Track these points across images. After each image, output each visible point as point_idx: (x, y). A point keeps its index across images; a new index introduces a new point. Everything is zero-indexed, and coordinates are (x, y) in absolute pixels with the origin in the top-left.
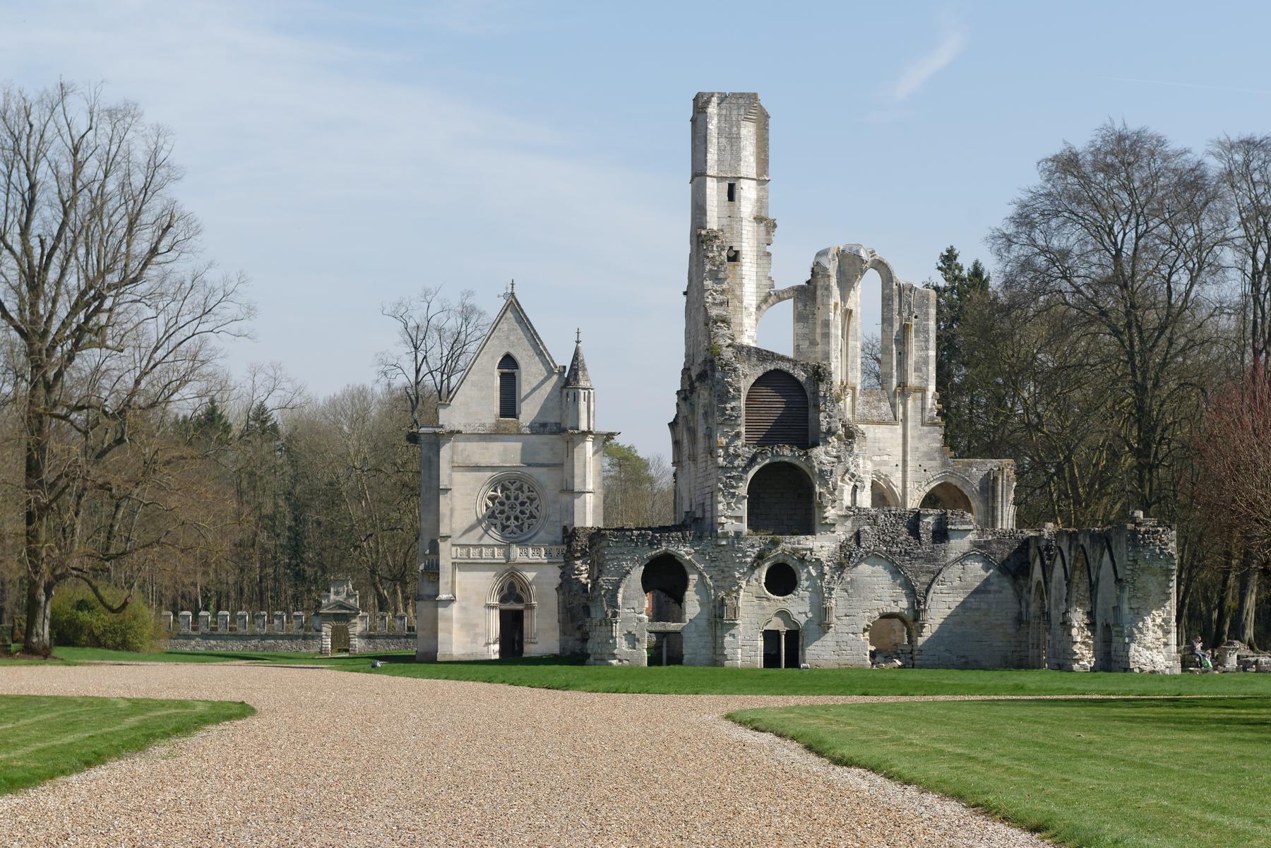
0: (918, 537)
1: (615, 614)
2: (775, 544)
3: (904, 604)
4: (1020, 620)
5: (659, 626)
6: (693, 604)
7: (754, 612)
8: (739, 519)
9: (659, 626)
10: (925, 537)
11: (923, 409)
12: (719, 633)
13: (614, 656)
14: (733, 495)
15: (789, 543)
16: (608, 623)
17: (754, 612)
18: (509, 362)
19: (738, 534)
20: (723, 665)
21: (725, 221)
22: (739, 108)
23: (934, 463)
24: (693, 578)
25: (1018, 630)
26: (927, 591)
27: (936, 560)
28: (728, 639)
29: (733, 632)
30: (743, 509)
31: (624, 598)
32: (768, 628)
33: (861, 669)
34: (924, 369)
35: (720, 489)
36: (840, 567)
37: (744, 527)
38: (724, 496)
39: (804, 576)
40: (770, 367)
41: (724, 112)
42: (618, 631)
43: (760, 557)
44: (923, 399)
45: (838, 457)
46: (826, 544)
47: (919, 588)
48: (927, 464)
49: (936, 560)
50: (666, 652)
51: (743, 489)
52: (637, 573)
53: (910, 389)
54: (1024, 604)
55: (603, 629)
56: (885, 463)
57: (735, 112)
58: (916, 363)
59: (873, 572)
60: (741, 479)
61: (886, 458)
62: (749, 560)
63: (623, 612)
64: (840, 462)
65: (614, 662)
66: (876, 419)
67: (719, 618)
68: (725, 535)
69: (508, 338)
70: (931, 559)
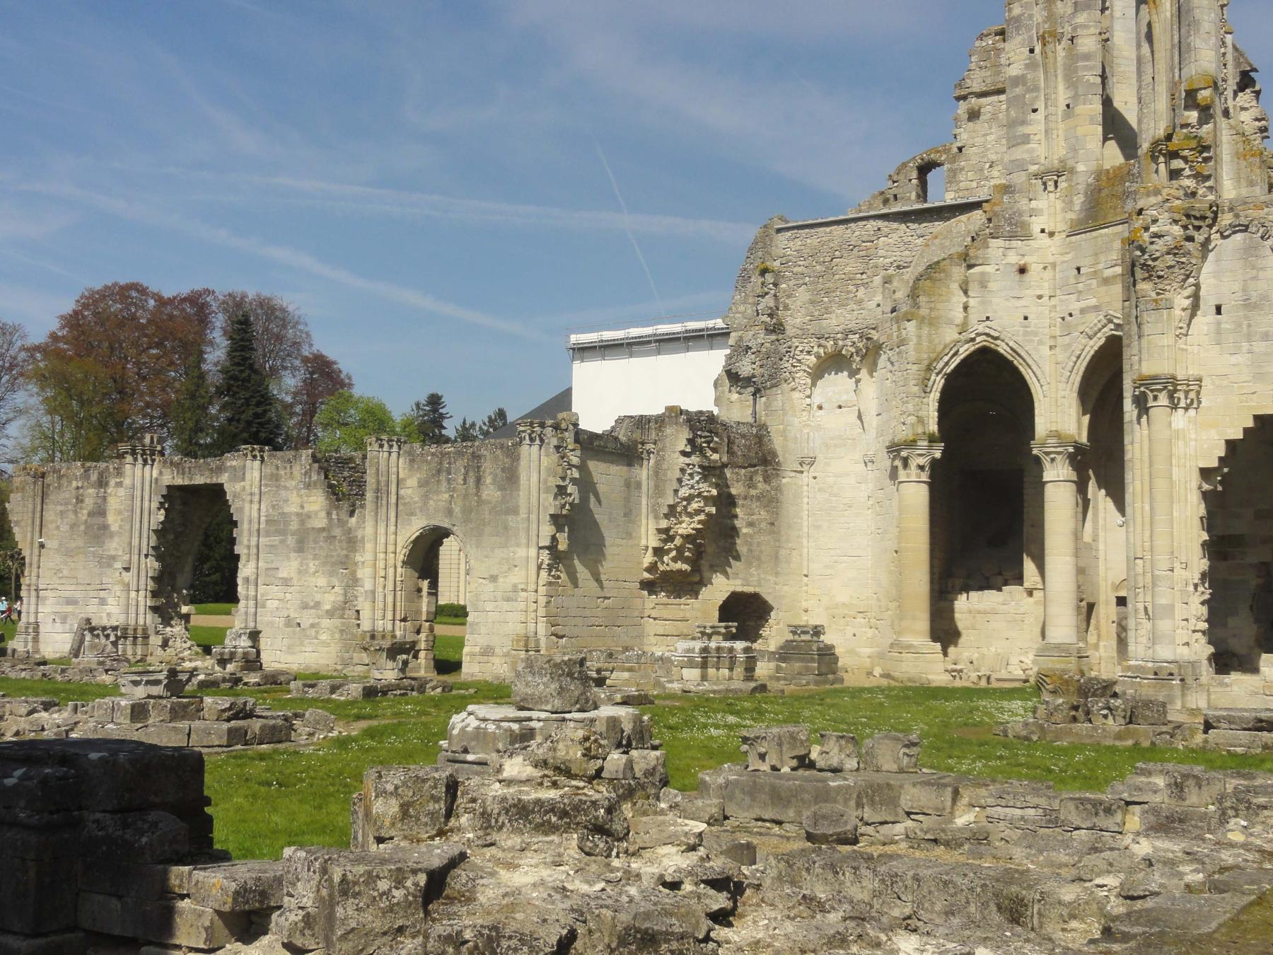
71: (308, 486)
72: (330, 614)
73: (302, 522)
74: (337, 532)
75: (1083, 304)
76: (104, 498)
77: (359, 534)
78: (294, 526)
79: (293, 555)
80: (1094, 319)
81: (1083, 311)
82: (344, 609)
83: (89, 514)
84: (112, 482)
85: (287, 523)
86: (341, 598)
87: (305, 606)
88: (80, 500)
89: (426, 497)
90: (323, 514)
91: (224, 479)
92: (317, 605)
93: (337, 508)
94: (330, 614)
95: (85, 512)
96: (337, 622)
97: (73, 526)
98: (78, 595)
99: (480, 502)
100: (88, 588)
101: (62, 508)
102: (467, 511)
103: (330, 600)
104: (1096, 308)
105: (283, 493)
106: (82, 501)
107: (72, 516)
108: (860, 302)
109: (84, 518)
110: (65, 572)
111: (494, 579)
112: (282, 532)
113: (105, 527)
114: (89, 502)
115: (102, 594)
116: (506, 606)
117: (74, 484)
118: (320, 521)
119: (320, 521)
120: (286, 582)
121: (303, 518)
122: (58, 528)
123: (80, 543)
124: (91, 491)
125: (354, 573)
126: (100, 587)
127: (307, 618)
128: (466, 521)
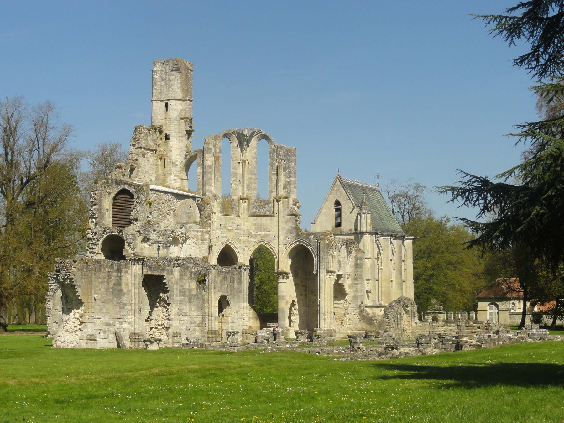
11: (287, 207)
18: (338, 203)
21: (163, 121)
22: (169, 66)
23: (292, 235)
31: (54, 304)
34: (288, 187)
35: (88, 250)
40: (121, 188)
41: (164, 69)
44: (288, 203)
45: (139, 231)
48: (289, 235)
53: (281, 198)
56: (267, 236)
57: (168, 69)
58: (285, 184)
61: (268, 233)
64: (140, 234)
66: (262, 214)
69: (336, 193)
71: (191, 279)
72: (199, 325)
73: (190, 292)
74: (200, 296)
75: (222, 235)
76: (120, 278)
77: (206, 297)
78: (187, 293)
79: (187, 304)
80: (225, 240)
81: (222, 237)
82: (202, 323)
83: (114, 284)
84: (124, 270)
85: (185, 292)
86: (201, 320)
87: (191, 323)
88: (110, 277)
89: (221, 286)
90: (196, 290)
91: (165, 274)
92: (195, 322)
93: (199, 288)
94: (199, 325)
95: (112, 283)
96: (200, 328)
97: (107, 289)
98: (111, 321)
99: (234, 288)
100: (115, 317)
101: (102, 280)
102: (231, 291)
103: (198, 320)
104: (226, 237)
105: (184, 281)
106: (111, 278)
107: (106, 285)
108: (168, 220)
109: (112, 286)
110: (104, 310)
111: (237, 312)
112: (184, 296)
113: (121, 290)
114: (114, 279)
115: (121, 320)
116: (240, 320)
117: (107, 270)
118: (195, 293)
119: (195, 293)
120: (186, 314)
121: (190, 290)
122: (100, 290)
123: (111, 297)
124: (115, 274)
125: (204, 311)
126: (119, 317)
127: (192, 327)
128: (231, 294)
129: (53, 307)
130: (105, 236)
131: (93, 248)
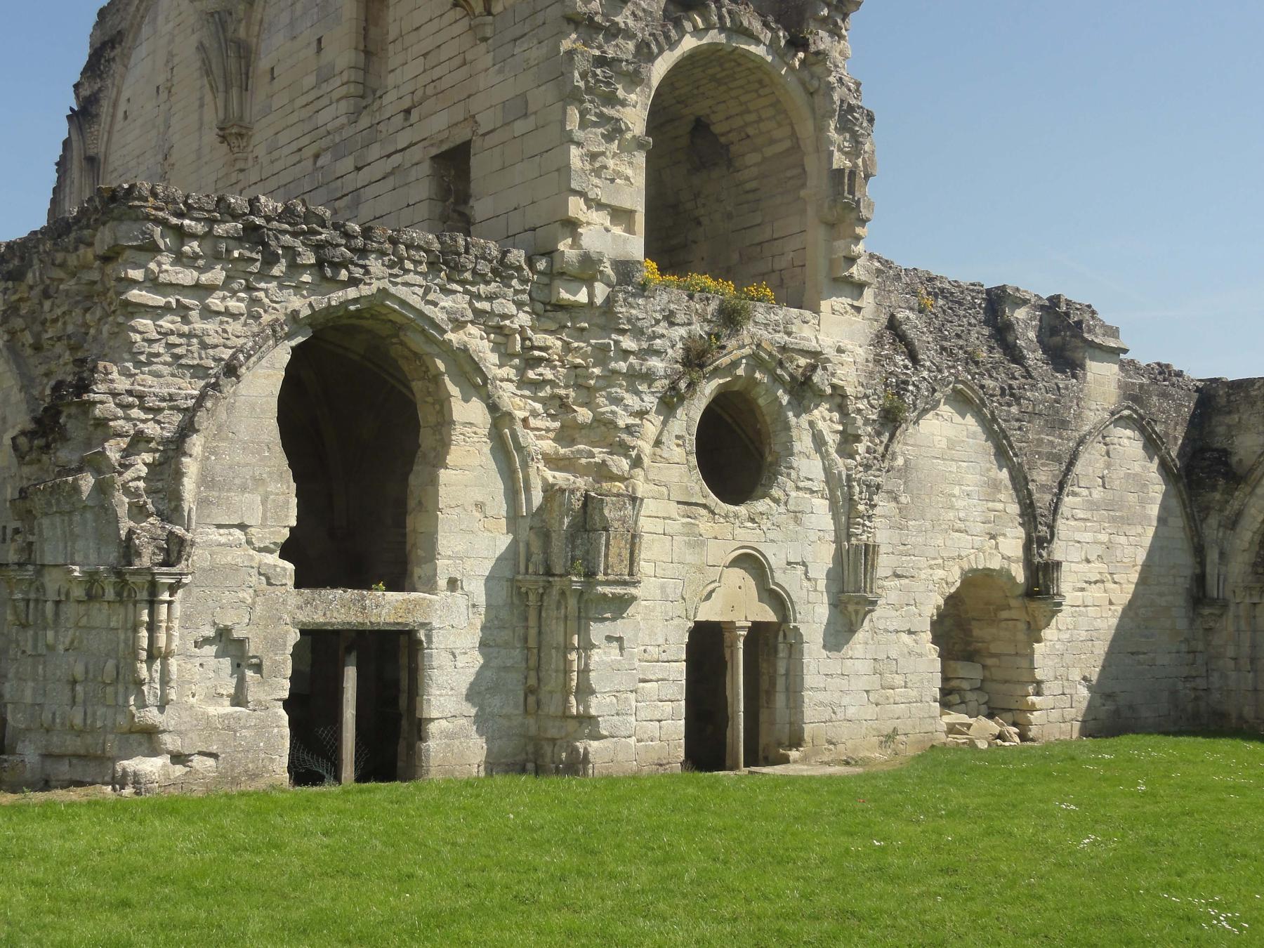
0: (1015, 356)
1: (174, 550)
2: (731, 318)
3: (1012, 543)
4: (1199, 595)
5: (339, 607)
6: (468, 522)
7: (681, 559)
8: (620, 215)
9: (339, 607)
10: (1034, 357)
12: (555, 631)
13: (148, 739)
14: (615, 130)
15: (768, 324)
16: (133, 585)
17: (681, 559)
19: (625, 269)
20: (576, 765)
24: (468, 413)
25: (1192, 622)
26: (1055, 511)
27: (1064, 424)
28: (602, 656)
29: (618, 628)
30: (629, 181)
31: (207, 480)
32: (709, 613)
33: (932, 754)
36: (891, 419)
37: (635, 246)
38: (583, 125)
39: (803, 442)
42: (180, 623)
43: (696, 359)
46: (847, 344)
47: (1043, 500)
49: (1064, 424)
50: (354, 708)
51: (635, 114)
52: (264, 381)
54: (1213, 556)
55: (99, 614)
59: (952, 445)
60: (635, 79)
62: (656, 364)
63: (209, 541)
65: (151, 766)
67: (562, 573)
68: (588, 270)
70: (1059, 424)
129: (203, 502)
130: (689, 43)
131: (612, 100)
